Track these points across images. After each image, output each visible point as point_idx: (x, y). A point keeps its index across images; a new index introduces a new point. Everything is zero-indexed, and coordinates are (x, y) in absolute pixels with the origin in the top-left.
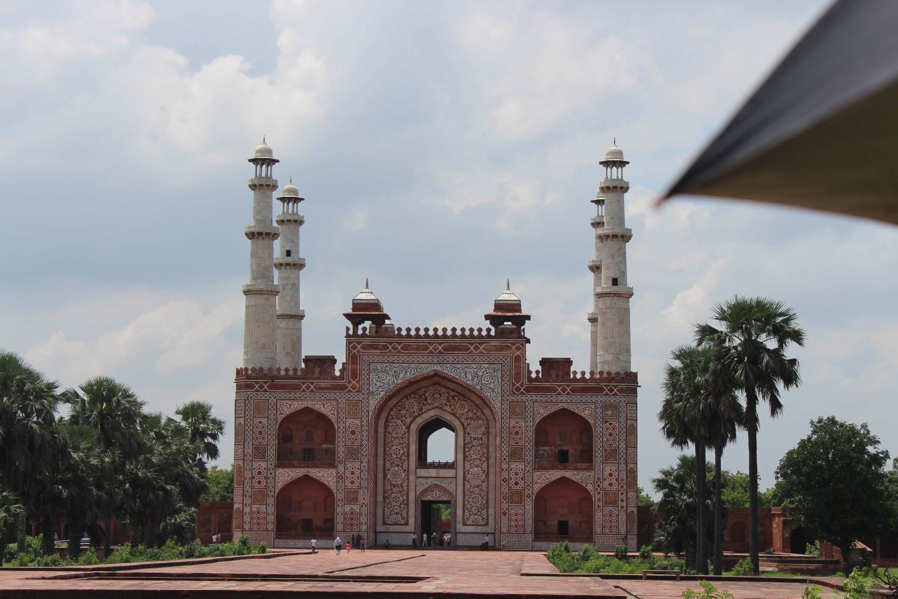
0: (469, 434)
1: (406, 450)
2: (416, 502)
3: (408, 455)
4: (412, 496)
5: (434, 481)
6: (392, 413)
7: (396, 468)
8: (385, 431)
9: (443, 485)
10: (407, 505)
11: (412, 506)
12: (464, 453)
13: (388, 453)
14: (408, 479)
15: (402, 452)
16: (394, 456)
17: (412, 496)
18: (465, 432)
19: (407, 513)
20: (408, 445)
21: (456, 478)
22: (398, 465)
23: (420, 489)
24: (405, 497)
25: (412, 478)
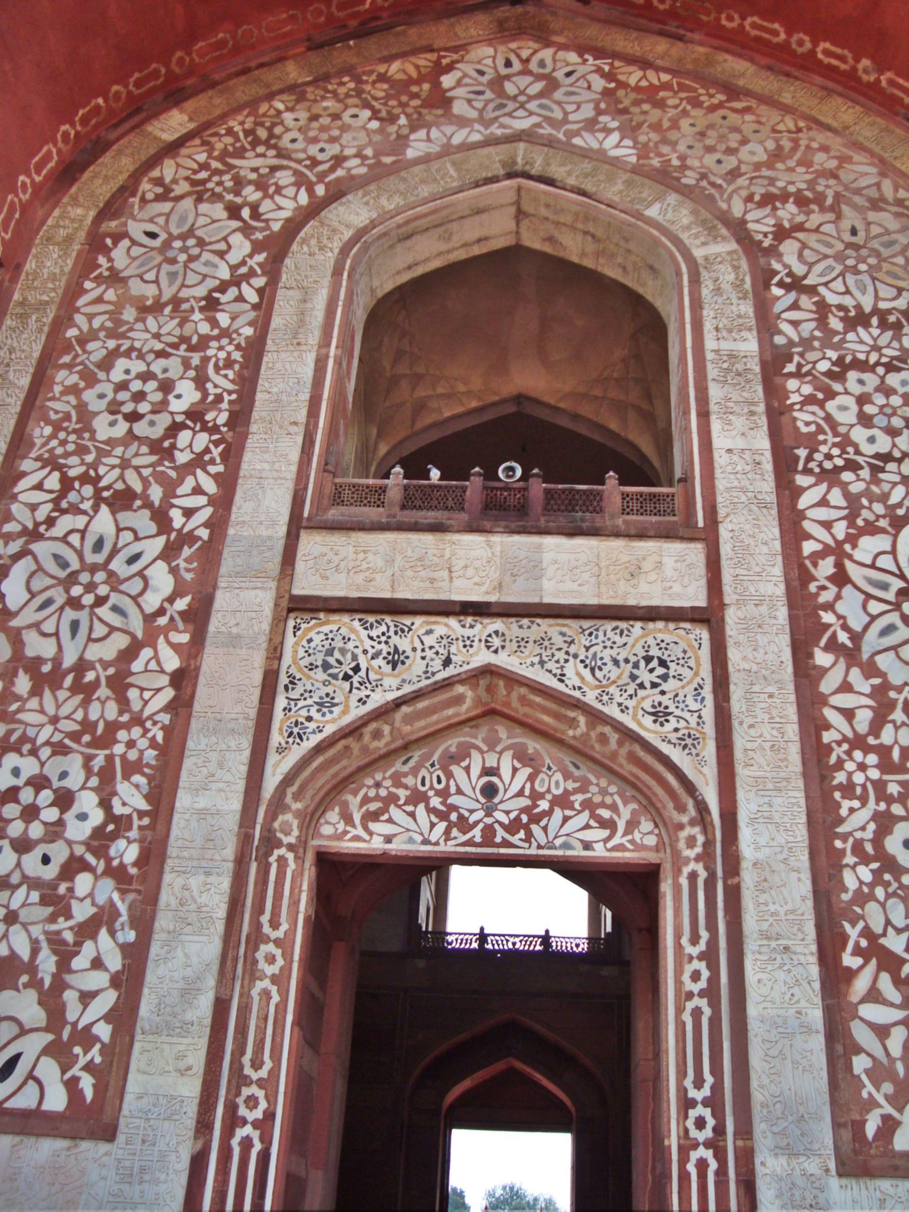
0: (795, 284)
1: (222, 382)
2: (253, 849)
3: (240, 418)
4: (210, 797)
5: (476, 646)
6: (168, 170)
7: (104, 522)
8: (86, 266)
9: (575, 679)
10: (144, 881)
11: (197, 890)
12: (777, 415)
13: (60, 406)
14: (198, 617)
15: (186, 395)
16: (106, 428)
17: (210, 797)
18: (764, 278)
19: (130, 980)
20: (255, 351)
21: (709, 616)
22: (122, 500)
23: (320, 713)
24: (131, 797)
25: (244, 604)
